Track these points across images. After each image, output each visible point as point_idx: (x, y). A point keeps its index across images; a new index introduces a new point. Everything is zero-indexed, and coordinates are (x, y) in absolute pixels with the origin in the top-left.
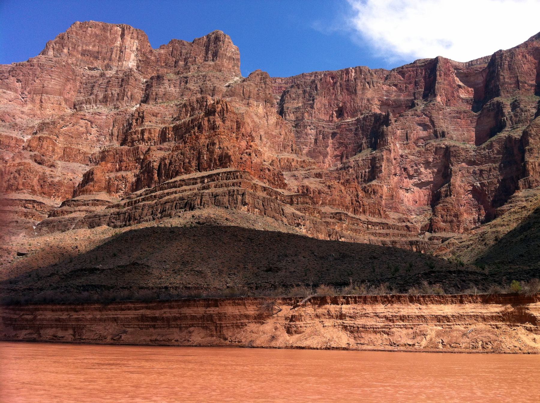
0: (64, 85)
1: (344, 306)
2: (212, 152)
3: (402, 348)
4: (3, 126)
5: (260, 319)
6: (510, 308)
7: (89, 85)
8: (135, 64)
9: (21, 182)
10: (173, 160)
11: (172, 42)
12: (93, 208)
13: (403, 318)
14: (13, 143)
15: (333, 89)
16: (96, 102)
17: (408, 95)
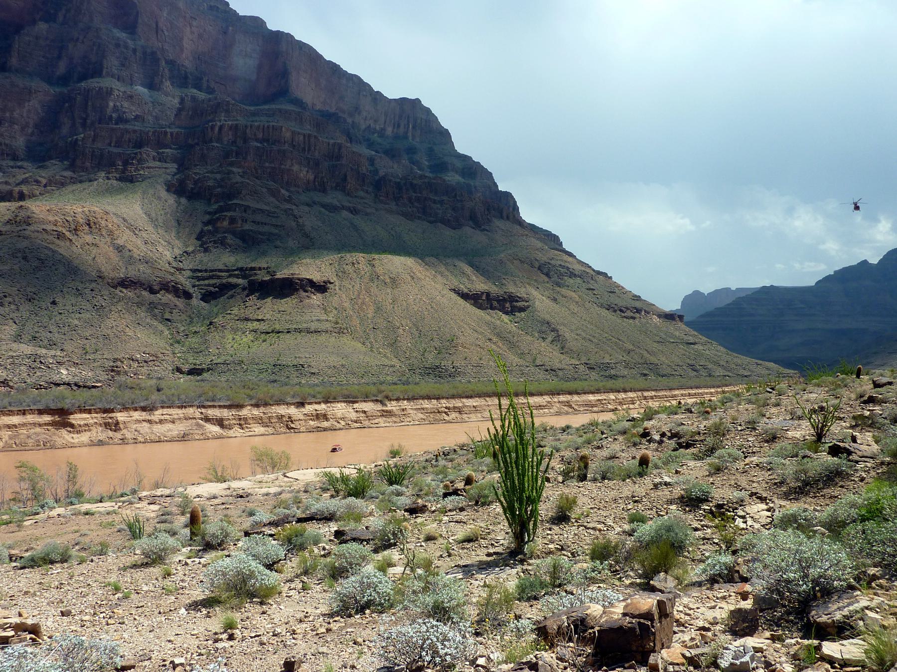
6: (57, 418)
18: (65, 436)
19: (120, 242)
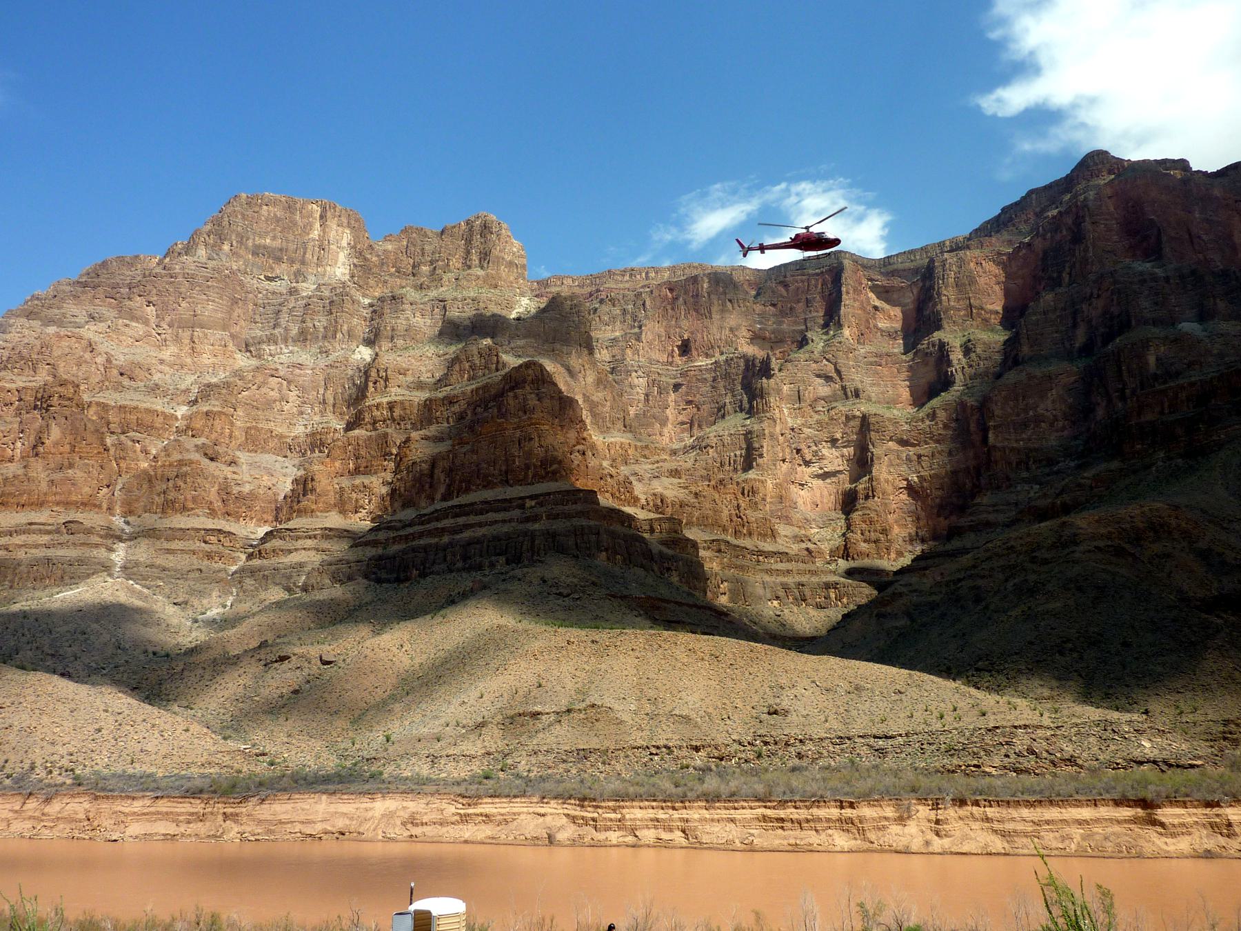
0: (230, 311)
1: (987, 809)
2: (529, 454)
3: (1056, 852)
4: (136, 390)
5: (901, 820)
6: (1140, 812)
7: (270, 309)
8: (347, 271)
9: (189, 497)
10: (458, 462)
11: (405, 231)
13: (1048, 822)
15: (673, 309)
16: (285, 341)
17: (795, 323)
18: (1153, 840)
19: (1202, 545)
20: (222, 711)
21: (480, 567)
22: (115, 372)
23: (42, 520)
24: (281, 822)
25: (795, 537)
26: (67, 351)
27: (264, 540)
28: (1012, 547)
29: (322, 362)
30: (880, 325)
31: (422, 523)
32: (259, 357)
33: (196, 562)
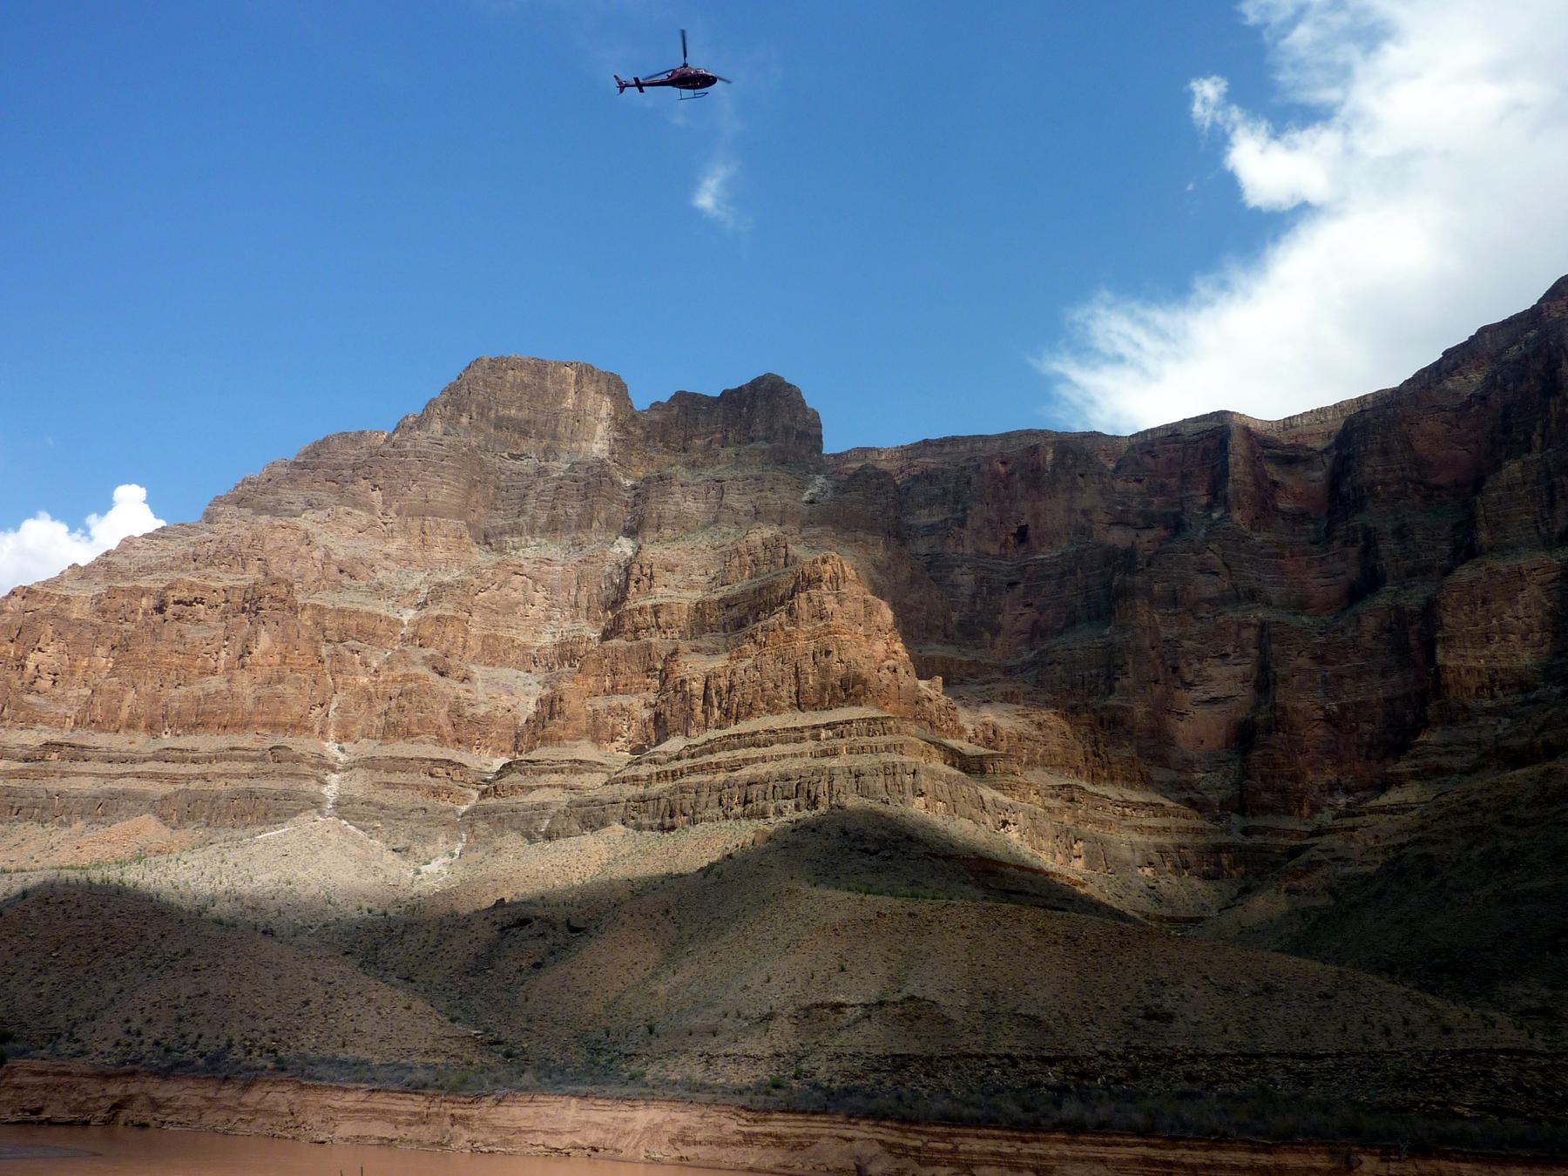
1: (1461, 1165)
2: (825, 671)
4: (357, 590)
7: (514, 493)
9: (414, 720)
10: (736, 681)
12: (575, 780)
14: (382, 628)
15: (1006, 488)
16: (531, 531)
20: (449, 986)
21: (763, 815)
22: (334, 568)
23: (245, 745)
24: (520, 1131)
25: (1172, 783)
26: (281, 543)
27: (500, 773)
28: (1476, 802)
29: (575, 558)
30: (1281, 505)
31: (693, 756)
32: (501, 551)
33: (420, 800)
